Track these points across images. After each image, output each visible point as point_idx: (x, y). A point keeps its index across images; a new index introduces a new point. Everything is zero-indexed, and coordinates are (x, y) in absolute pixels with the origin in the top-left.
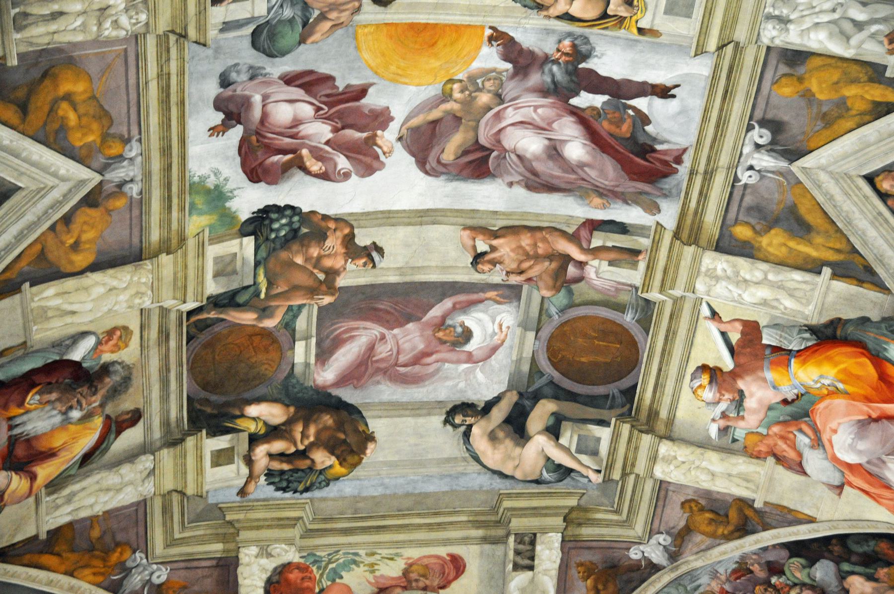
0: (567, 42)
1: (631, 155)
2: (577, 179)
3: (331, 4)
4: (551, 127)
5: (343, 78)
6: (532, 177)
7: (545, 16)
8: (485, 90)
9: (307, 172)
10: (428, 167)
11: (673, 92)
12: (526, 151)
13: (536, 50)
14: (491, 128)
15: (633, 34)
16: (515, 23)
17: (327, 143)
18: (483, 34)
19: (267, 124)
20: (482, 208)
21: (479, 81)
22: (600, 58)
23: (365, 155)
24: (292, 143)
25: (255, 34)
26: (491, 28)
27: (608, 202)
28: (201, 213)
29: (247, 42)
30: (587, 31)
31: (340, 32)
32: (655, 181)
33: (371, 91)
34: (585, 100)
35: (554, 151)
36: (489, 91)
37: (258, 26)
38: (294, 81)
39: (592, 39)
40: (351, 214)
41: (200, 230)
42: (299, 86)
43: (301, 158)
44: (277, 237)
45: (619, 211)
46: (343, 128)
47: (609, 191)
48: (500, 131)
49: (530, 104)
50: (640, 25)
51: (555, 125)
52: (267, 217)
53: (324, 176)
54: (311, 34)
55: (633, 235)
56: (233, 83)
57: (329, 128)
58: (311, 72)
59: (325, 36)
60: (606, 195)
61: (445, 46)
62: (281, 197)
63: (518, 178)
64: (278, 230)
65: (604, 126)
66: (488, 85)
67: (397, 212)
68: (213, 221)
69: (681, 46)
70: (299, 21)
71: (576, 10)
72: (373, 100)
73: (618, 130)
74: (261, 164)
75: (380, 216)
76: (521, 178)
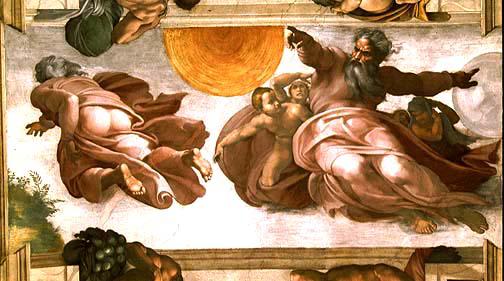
0: (363, 40)
1: (447, 162)
2: (398, 200)
3: (139, 4)
4: (364, 141)
5: (156, 86)
6: (353, 203)
7: (338, 13)
8: (293, 100)
9: (129, 193)
10: (248, 193)
11: (473, 79)
12: (342, 171)
13: (336, 50)
14: (305, 146)
15: (422, 19)
16: (312, 22)
17: (146, 160)
18: (283, 35)
19: (84, 130)
20: (308, 245)
21: (286, 89)
22: (397, 53)
23: (182, 176)
24: (111, 155)
25: (69, 28)
26: (289, 28)
27: (433, 223)
28: (21, 225)
29: (61, 35)
30: (381, 25)
31: (149, 33)
32: (476, 188)
33: (184, 102)
34: (393, 103)
35: (370, 167)
36: (297, 101)
37: (71, 20)
38: (111, 83)
39: (387, 33)
40: (177, 252)
41: (21, 246)
42: (112, 91)
43: (119, 173)
44: (102, 271)
45: (447, 234)
46: (160, 145)
47: (433, 208)
48: (315, 148)
49: (340, 114)
50: (428, 10)
51: (367, 138)
52: (91, 243)
53: (146, 199)
54: (122, 34)
55: (463, 262)
56: (50, 78)
57: (147, 143)
58: (125, 76)
59: (135, 37)
60: (431, 216)
61: (249, 50)
62: (104, 219)
63: (339, 205)
64: (102, 262)
65: (415, 132)
66: (295, 92)
67: (224, 251)
68: (34, 237)
69: (471, 25)
70: (110, 18)
71: (367, 4)
72: (188, 112)
73: (429, 134)
74: (81, 175)
75: (207, 256)
76: (343, 205)
